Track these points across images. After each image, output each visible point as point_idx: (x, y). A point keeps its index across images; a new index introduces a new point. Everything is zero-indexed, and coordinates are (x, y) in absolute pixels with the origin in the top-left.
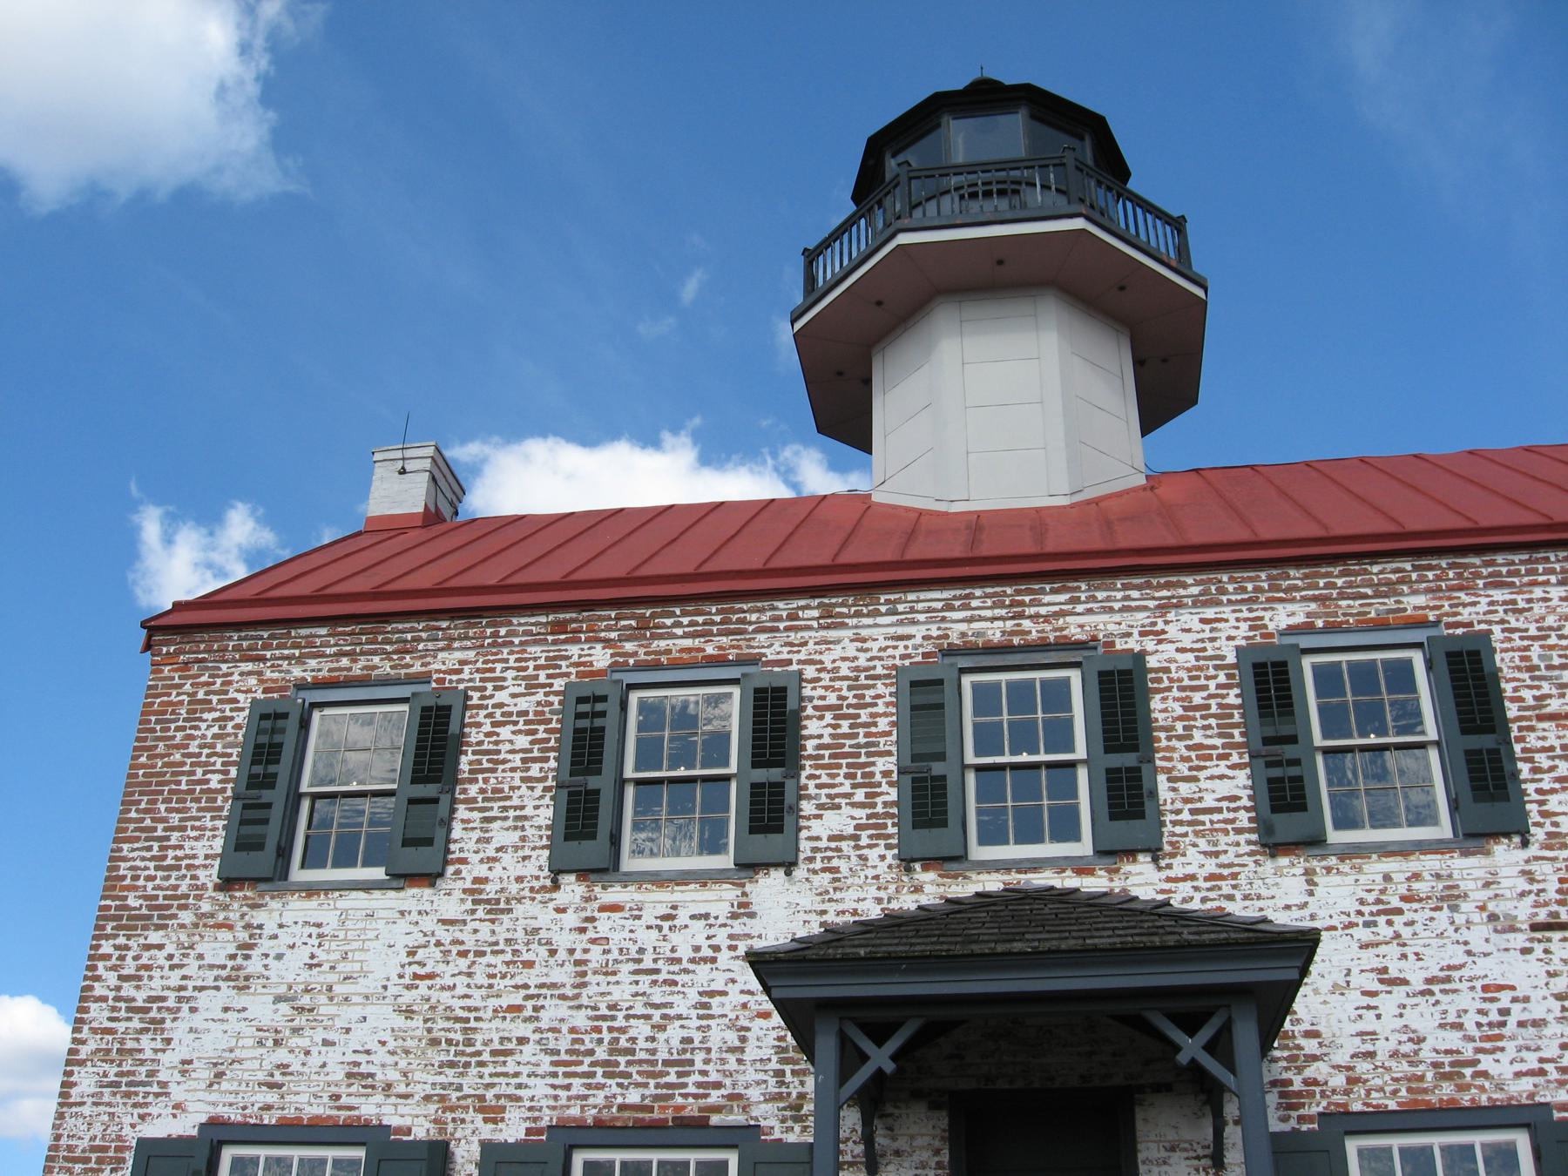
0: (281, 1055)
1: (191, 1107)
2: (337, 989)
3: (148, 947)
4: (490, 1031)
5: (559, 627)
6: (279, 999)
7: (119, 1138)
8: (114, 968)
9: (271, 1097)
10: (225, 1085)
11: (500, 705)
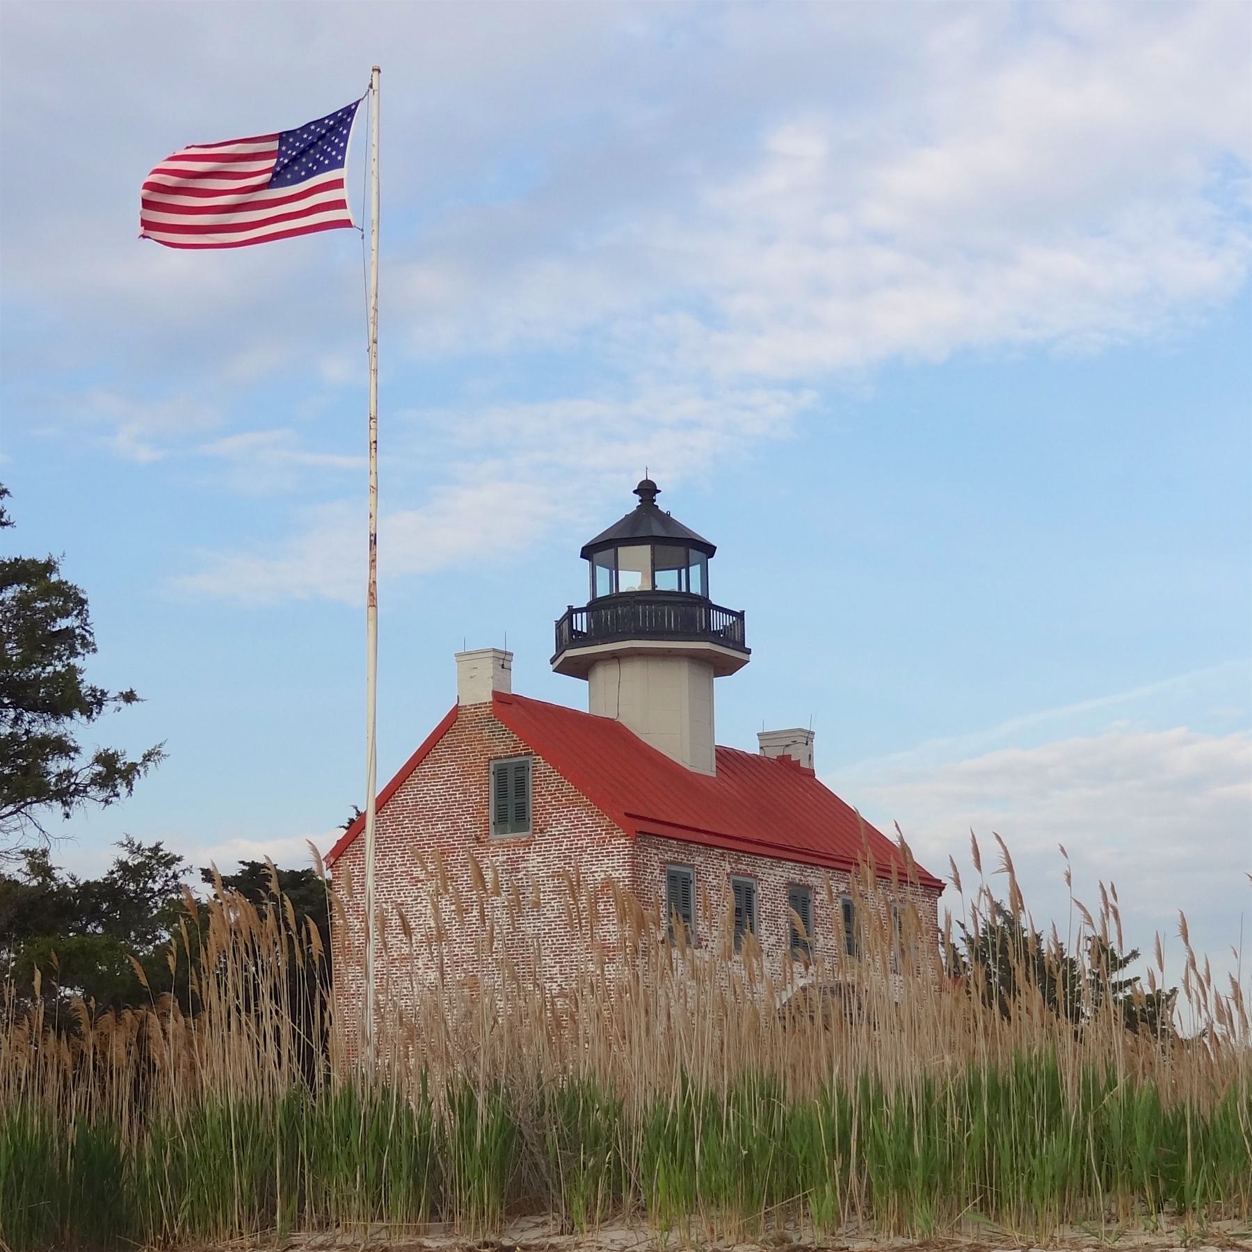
11: (710, 882)
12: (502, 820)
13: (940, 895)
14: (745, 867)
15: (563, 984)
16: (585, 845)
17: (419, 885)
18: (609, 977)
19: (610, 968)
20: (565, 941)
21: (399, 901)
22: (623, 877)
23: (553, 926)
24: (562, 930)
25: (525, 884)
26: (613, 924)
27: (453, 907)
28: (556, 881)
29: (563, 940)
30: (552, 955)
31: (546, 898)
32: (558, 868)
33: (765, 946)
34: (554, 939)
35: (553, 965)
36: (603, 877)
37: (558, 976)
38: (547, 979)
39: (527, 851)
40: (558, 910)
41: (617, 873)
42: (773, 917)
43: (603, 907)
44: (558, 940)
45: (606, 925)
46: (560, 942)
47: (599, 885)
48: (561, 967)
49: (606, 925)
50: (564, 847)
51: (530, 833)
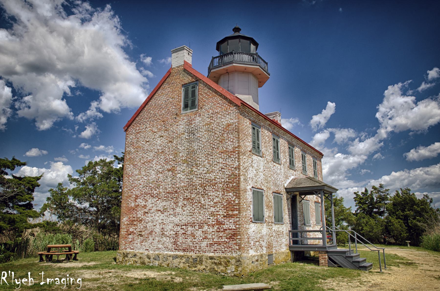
0: (256, 179)
1: (251, 184)
2: (259, 170)
3: (245, 159)
4: (269, 179)
5: (270, 125)
6: (255, 170)
7: (246, 188)
8: (242, 161)
9: (256, 184)
10: (253, 182)
12: (186, 106)
13: (322, 157)
14: (276, 132)
15: (209, 168)
16: (219, 111)
17: (155, 134)
18: (229, 164)
19: (229, 160)
20: (210, 150)
21: (148, 140)
22: (235, 122)
23: (205, 145)
24: (209, 146)
25: (194, 129)
26: (230, 142)
27: (167, 141)
28: (207, 127)
29: (209, 150)
30: (204, 156)
31: (203, 134)
32: (207, 121)
33: (282, 162)
34: (206, 150)
35: (205, 160)
36: (226, 123)
37: (207, 165)
38: (202, 166)
39: (195, 116)
40: (207, 138)
41: (232, 121)
42: (284, 152)
43: (226, 135)
44: (207, 150)
45: (228, 142)
46: (208, 151)
47: (225, 127)
48: (208, 161)
49: (228, 142)
50: (210, 113)
51: (197, 109)
